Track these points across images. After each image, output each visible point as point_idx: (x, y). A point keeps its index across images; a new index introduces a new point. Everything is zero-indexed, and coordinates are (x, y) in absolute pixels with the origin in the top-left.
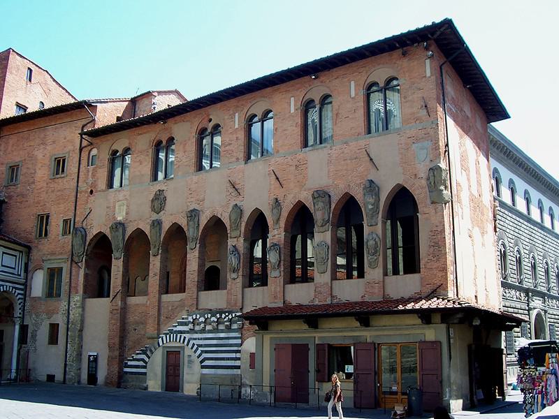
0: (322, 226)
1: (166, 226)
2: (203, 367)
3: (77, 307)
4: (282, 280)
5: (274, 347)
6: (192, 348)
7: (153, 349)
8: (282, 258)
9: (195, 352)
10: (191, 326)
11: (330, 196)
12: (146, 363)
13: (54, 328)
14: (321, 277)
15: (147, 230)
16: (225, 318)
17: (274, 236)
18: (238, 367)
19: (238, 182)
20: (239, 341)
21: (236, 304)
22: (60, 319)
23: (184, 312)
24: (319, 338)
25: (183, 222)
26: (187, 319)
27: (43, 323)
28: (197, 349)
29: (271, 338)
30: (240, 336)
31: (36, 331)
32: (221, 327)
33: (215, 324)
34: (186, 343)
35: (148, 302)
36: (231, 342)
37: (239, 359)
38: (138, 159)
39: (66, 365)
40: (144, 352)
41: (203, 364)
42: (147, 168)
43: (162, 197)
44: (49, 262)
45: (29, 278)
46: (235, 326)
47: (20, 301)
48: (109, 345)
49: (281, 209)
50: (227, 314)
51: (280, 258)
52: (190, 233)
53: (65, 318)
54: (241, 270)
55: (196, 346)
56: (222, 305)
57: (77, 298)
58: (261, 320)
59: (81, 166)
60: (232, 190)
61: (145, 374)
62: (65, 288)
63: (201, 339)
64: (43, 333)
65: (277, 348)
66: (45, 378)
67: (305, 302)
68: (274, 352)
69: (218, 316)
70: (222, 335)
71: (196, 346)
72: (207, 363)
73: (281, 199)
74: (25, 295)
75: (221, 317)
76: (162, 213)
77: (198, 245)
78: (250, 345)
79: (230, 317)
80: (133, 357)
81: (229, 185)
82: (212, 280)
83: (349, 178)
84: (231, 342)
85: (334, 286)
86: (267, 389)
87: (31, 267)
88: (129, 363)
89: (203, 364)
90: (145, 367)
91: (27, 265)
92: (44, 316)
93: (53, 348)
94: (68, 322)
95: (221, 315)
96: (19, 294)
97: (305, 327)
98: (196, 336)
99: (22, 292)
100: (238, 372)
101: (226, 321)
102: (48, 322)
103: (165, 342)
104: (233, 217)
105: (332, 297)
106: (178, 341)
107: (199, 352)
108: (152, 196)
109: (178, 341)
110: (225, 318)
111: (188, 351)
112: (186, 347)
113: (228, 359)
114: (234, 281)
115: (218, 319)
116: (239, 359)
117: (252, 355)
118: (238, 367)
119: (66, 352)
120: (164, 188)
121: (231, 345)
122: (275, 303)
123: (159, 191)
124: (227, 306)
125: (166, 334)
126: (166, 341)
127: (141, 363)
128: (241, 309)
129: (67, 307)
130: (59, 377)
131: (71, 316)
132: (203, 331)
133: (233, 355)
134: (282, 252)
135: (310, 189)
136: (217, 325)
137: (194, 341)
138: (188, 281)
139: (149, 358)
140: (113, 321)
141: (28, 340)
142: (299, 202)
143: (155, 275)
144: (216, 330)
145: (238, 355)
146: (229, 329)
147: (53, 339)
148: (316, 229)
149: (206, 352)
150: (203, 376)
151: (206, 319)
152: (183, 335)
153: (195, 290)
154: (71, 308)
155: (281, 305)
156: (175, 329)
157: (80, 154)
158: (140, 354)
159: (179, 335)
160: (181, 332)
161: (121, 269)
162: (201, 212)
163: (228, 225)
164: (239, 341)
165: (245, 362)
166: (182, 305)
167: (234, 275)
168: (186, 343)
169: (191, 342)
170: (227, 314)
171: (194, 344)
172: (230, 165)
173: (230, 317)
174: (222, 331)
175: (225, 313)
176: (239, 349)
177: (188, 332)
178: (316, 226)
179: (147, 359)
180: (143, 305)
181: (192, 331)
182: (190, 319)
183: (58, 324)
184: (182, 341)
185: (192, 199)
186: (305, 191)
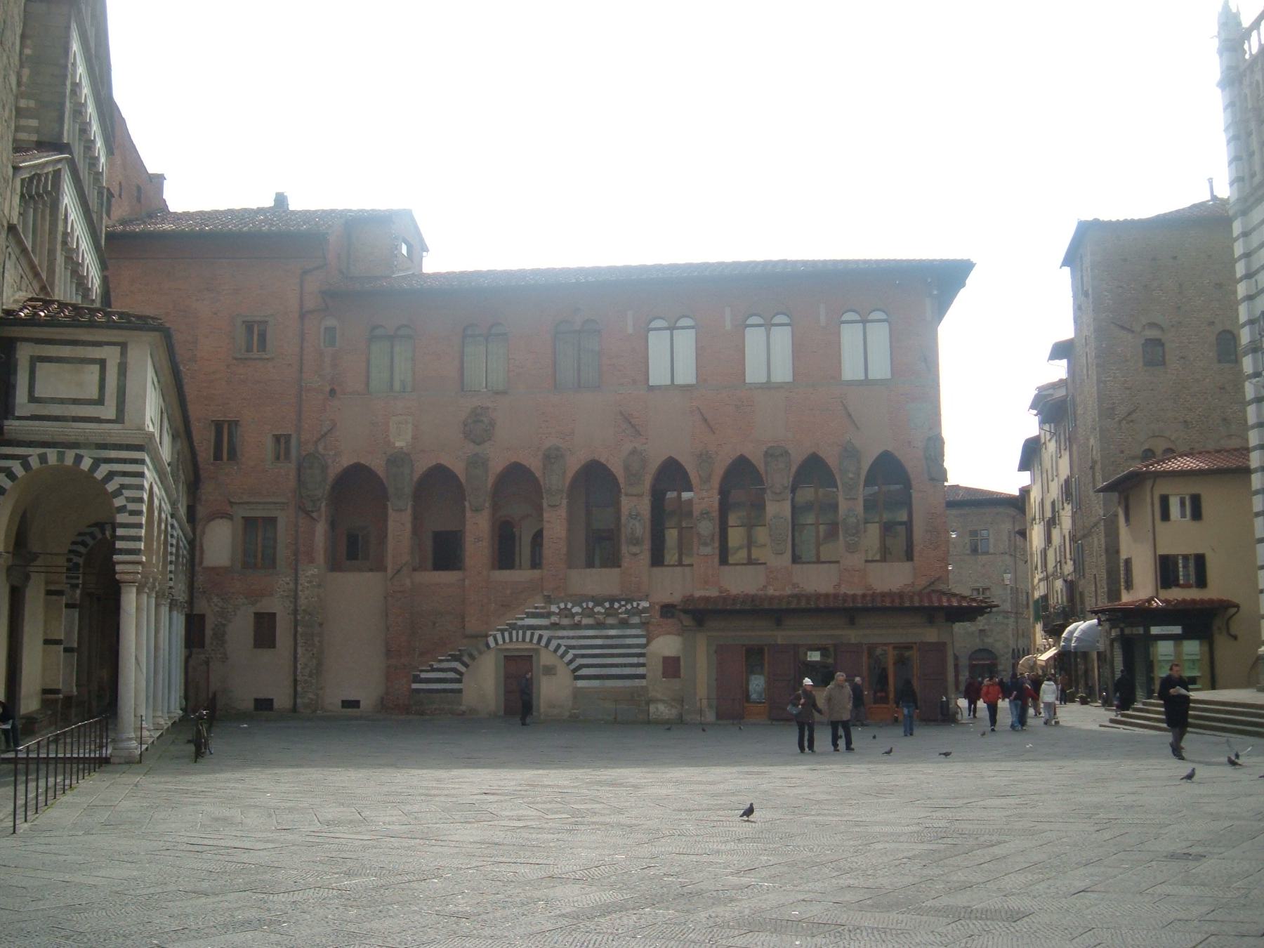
1: (498, 463)
2: (577, 678)
6: (556, 651)
7: (475, 653)
9: (562, 656)
10: (554, 619)
12: (461, 674)
15: (458, 468)
18: (643, 677)
20: (643, 641)
22: (277, 605)
28: (566, 652)
31: (224, 625)
32: (610, 621)
34: (543, 643)
35: (467, 582)
36: (628, 641)
37: (643, 665)
39: (295, 681)
40: (455, 658)
45: (198, 532)
46: (635, 620)
55: (563, 649)
56: (616, 591)
61: (460, 691)
62: (283, 552)
63: (573, 638)
64: (241, 628)
66: (251, 705)
69: (607, 605)
70: (613, 632)
71: (563, 649)
75: (612, 606)
77: (565, 502)
78: (667, 645)
79: (629, 607)
84: (628, 641)
86: (705, 702)
87: (201, 511)
88: (423, 675)
90: (459, 681)
91: (191, 511)
93: (266, 655)
94: (295, 612)
98: (565, 633)
100: (644, 682)
102: (252, 610)
103: (500, 641)
105: (795, 585)
106: (528, 639)
107: (569, 657)
109: (528, 639)
111: (546, 658)
113: (625, 665)
114: (636, 558)
116: (643, 665)
118: (643, 677)
121: (629, 646)
125: (502, 631)
126: (498, 640)
127: (451, 675)
129: (292, 586)
130: (282, 700)
131: (302, 601)
132: (577, 626)
133: (635, 660)
137: (560, 641)
139: (467, 666)
141: (208, 640)
144: (600, 625)
145: (642, 660)
146: (624, 624)
148: (768, 496)
149: (583, 656)
150: (577, 694)
152: (537, 633)
154: (300, 588)
155: (713, 593)
156: (520, 623)
159: (528, 633)
160: (533, 628)
161: (409, 526)
163: (621, 480)
164: (643, 641)
165: (654, 669)
167: (635, 549)
168: (543, 643)
169: (554, 643)
171: (559, 646)
173: (629, 607)
174: (612, 627)
175: (619, 601)
179: (463, 669)
181: (555, 626)
183: (274, 614)
184: (535, 641)
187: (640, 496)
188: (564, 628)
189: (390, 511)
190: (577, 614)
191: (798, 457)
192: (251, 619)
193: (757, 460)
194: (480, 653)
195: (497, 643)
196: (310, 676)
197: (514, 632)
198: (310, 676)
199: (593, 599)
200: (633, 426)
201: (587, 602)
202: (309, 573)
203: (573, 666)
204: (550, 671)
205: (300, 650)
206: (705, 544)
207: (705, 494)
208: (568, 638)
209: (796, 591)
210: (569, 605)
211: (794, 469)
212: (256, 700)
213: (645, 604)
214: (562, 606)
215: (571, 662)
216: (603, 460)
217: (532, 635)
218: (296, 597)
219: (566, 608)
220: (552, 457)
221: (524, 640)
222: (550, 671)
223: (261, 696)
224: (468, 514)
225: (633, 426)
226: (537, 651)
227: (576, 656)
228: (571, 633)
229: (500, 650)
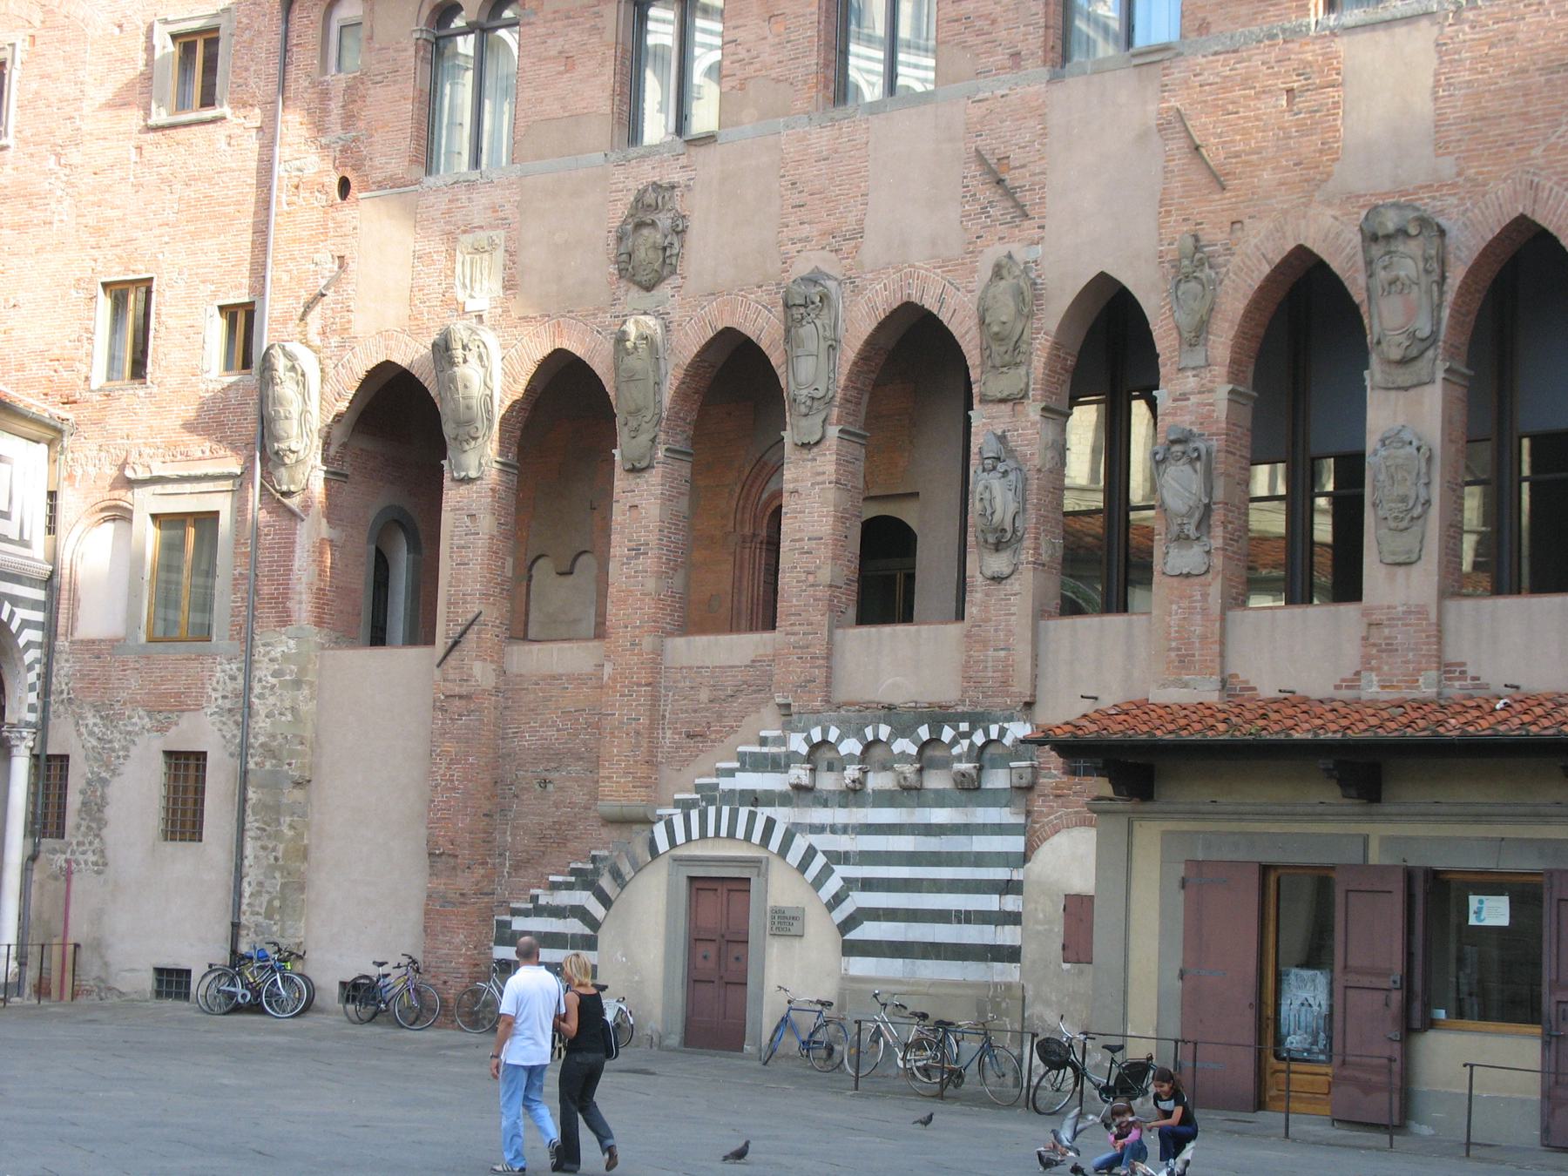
0: (1404, 362)
2: (852, 949)
3: (284, 685)
4: (1215, 590)
5: (1180, 870)
6: (803, 866)
7: (626, 868)
8: (1219, 494)
9: (818, 883)
10: (799, 774)
11: (1442, 233)
12: (594, 924)
13: (186, 768)
14: (1397, 583)
16: (954, 742)
17: (1184, 397)
18: (1011, 954)
19: (1016, 156)
20: (1016, 844)
21: (1005, 683)
22: (204, 731)
23: (769, 714)
24: (1385, 840)
25: (763, 328)
26: (782, 741)
27: (134, 751)
28: (826, 872)
29: (1165, 833)
30: (1021, 820)
31: (104, 782)
32: (937, 781)
33: (909, 769)
34: (775, 844)
35: (608, 669)
36: (981, 844)
37: (1014, 918)
38: (555, 45)
39: (236, 926)
40: (586, 881)
41: (851, 936)
42: (595, 90)
43: (664, 220)
44: (158, 489)
46: (998, 779)
47: (29, 657)
48: (431, 842)
50: (964, 727)
51: (1209, 491)
53: (232, 730)
54: (1028, 543)
55: (819, 861)
56: (943, 688)
57: (278, 646)
58: (1129, 766)
59: (293, 72)
60: (987, 193)
63: (845, 829)
64: (139, 789)
65: (1197, 881)
66: (148, 982)
67: (1316, 682)
68: (1180, 897)
69: (924, 732)
70: (940, 816)
71: (819, 861)
72: (869, 931)
73: (1215, 235)
74: (50, 628)
75: (935, 741)
76: (665, 289)
77: (833, 431)
78: (1070, 858)
80: (535, 898)
81: (974, 169)
82: (885, 578)
83: (1537, 152)
84: (981, 844)
85: (1451, 621)
89: (851, 936)
90: (590, 943)
92: (140, 719)
93: (182, 851)
95: (936, 729)
96: (26, 624)
97: (1331, 794)
99: (39, 616)
101: (959, 758)
103: (680, 837)
105: (1448, 669)
106: (740, 833)
107: (833, 885)
108: (621, 210)
109: (740, 833)
110: (954, 742)
112: (776, 863)
113: (966, 917)
114: (1010, 589)
115: (923, 746)
116: (1014, 918)
117: (1078, 909)
118: (1011, 954)
119: (239, 876)
120: (677, 177)
121: (979, 859)
122: (1186, 686)
123: (657, 187)
124: (964, 691)
125: (686, 806)
127: (574, 926)
128: (1029, 705)
131: (261, 724)
132: (854, 795)
133: (991, 902)
134: (1220, 468)
135: (1351, 197)
136: (920, 771)
138: (788, 580)
139: (606, 902)
140: (450, 747)
141: (71, 819)
142: (1301, 252)
143: (637, 551)
144: (910, 793)
145: (1011, 903)
146: (969, 789)
147: (183, 820)
148: (1374, 374)
149: (868, 885)
151: (868, 746)
152: (763, 813)
153: (820, 618)
154: (257, 689)
156: (725, 784)
157: (287, 21)
158: (569, 886)
159: (744, 813)
160: (755, 799)
163: (973, 357)
164: (1016, 844)
165: (1041, 933)
166: (756, 683)
167: (999, 563)
168: (775, 844)
169: (800, 844)
170: (964, 727)
171: (811, 853)
172: (981, 82)
173: (979, 738)
174: (940, 799)
175: (954, 720)
176: (1017, 875)
177: (783, 799)
178: (1374, 359)
179: (598, 910)
180: (579, 680)
181: (802, 793)
182: (797, 743)
183: (202, 756)
184: (757, 837)
185: (806, 230)
186: (1328, 203)
187: (1014, 400)
188: (825, 804)
189: (447, 482)
190: (850, 758)
191: (1471, 231)
192: (159, 765)
193: (1343, 256)
194: (638, 869)
195: (673, 843)
196: (269, 916)
197: (712, 810)
198: (269, 916)
199: (889, 712)
201: (876, 722)
202: (277, 652)
203: (840, 914)
204: (787, 924)
205: (250, 848)
206: (1182, 539)
208: (834, 829)
209: (1455, 689)
210: (833, 734)
211: (1456, 276)
212: (160, 971)
213: (1019, 730)
214: (817, 735)
215: (837, 900)
216: (930, 304)
217: (752, 817)
218: (248, 710)
219: (825, 742)
220: (804, 304)
221: (731, 835)
222: (787, 924)
223: (168, 962)
224: (621, 481)
225: (1009, 193)
226: (755, 863)
227: (850, 883)
228: (840, 816)
229: (676, 859)
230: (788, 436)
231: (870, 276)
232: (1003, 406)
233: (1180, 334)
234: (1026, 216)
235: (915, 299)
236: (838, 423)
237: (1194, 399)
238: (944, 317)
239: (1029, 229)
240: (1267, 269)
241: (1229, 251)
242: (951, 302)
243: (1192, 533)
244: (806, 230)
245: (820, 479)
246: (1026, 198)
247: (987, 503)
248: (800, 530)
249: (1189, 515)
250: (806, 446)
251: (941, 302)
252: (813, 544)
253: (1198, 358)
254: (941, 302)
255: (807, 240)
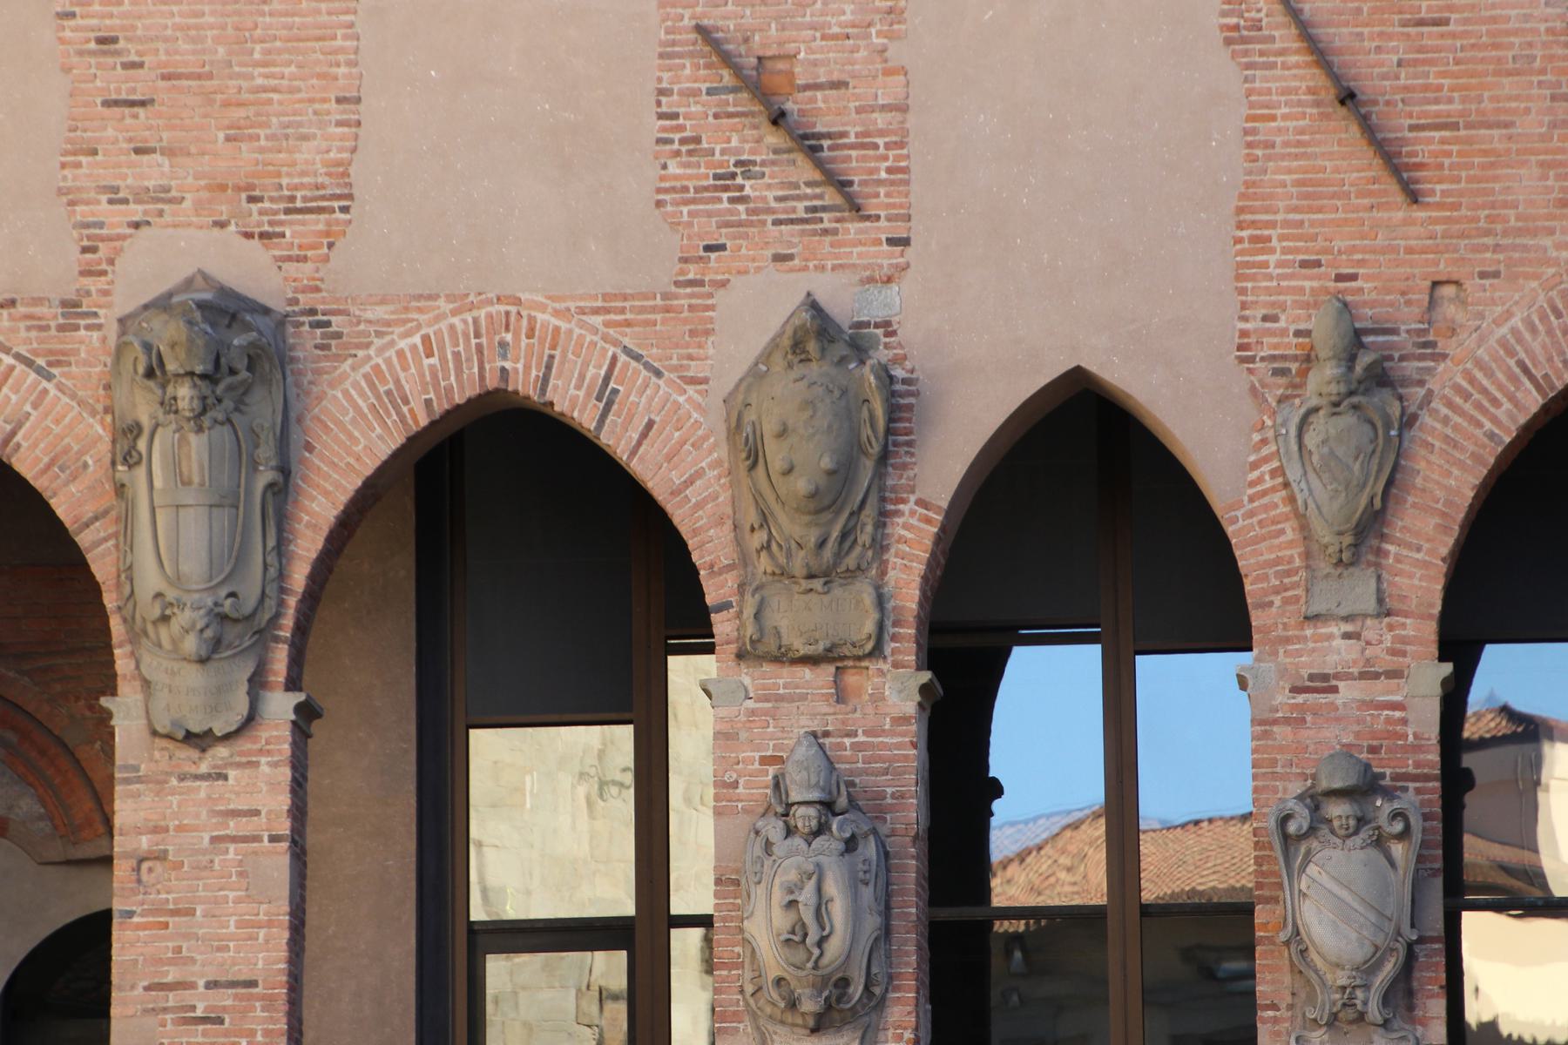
17: (1323, 683)
19: (812, 58)
49: (1408, 421)
52: (152, 541)
60: (747, 138)
77: (281, 705)
81: (692, 73)
104: (805, 458)
162: (305, 341)
185: (155, 170)
200: (809, 144)
207: (1336, 651)
216: (571, 400)
225: (809, 144)
230: (127, 713)
231: (381, 312)
232: (806, 673)
233: (1304, 528)
234: (855, 208)
235: (524, 384)
236: (292, 684)
237: (1348, 692)
238: (617, 440)
239: (861, 244)
240: (1533, 401)
241: (1429, 349)
242: (642, 397)
243: (1374, 1012)
244: (155, 170)
245: (233, 827)
246: (854, 165)
247: (808, 917)
248: (178, 958)
249: (1369, 968)
250: (199, 740)
251: (607, 398)
252: (226, 998)
253: (1359, 590)
254: (607, 398)
255: (163, 195)
